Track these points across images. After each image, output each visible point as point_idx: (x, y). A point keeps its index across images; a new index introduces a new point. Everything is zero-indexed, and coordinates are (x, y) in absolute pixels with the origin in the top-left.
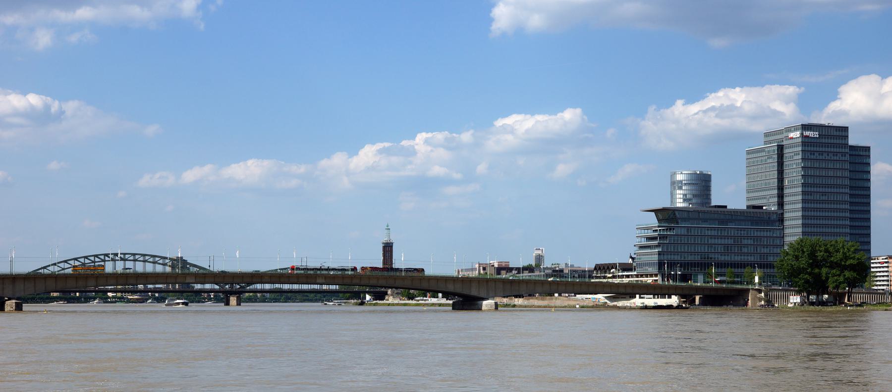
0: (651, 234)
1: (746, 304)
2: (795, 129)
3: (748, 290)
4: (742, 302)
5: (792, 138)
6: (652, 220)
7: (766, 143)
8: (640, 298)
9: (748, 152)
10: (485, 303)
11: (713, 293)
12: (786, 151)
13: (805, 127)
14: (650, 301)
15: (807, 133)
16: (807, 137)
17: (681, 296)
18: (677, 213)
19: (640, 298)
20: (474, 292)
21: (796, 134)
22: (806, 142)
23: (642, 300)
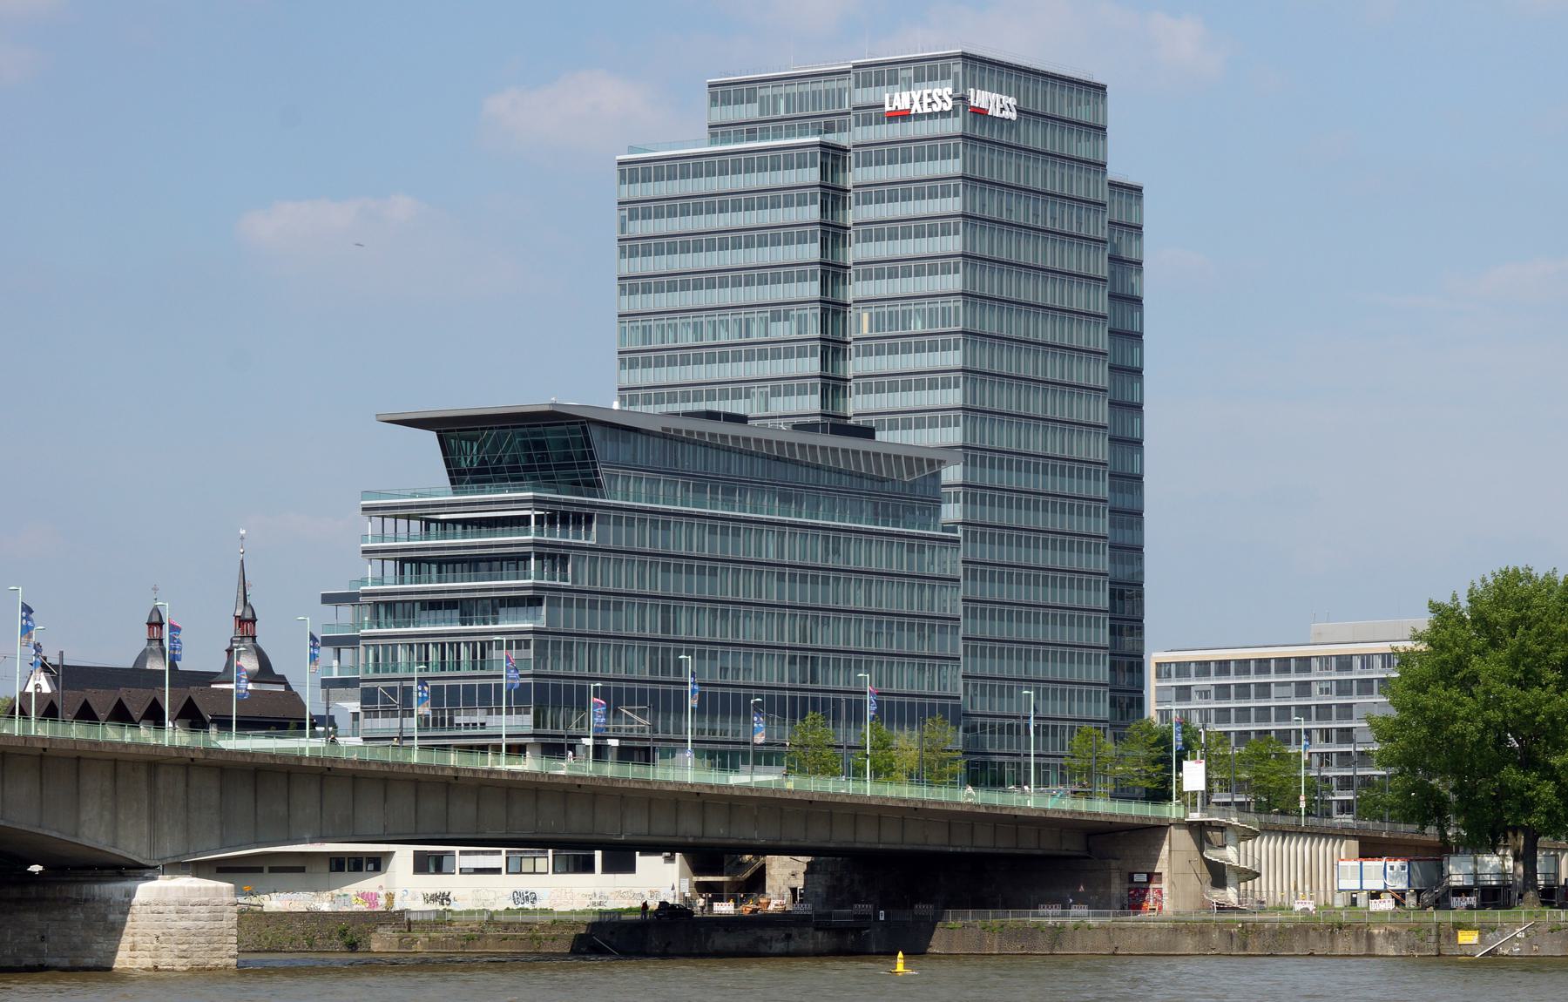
0: (411, 538)
1: (1135, 900)
2: (927, 69)
3: (1153, 833)
4: (1117, 888)
5: (904, 116)
6: (422, 469)
7: (718, 130)
8: (423, 865)
9: (631, 171)
10: (146, 891)
11: (1004, 845)
12: (855, 176)
13: (979, 67)
14: (483, 886)
15: (981, 98)
16: (979, 113)
17: (703, 858)
18: (595, 434)
19: (423, 865)
20: (94, 831)
21: (941, 95)
22: (980, 132)
23: (433, 883)
